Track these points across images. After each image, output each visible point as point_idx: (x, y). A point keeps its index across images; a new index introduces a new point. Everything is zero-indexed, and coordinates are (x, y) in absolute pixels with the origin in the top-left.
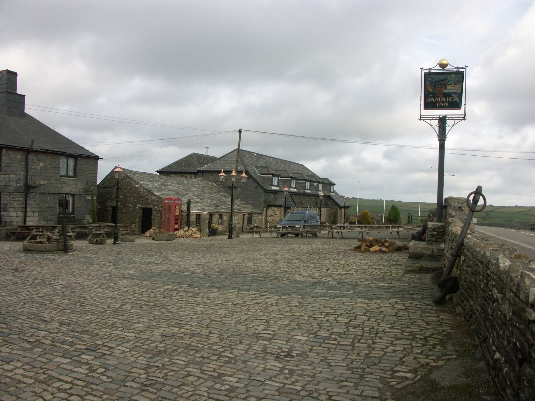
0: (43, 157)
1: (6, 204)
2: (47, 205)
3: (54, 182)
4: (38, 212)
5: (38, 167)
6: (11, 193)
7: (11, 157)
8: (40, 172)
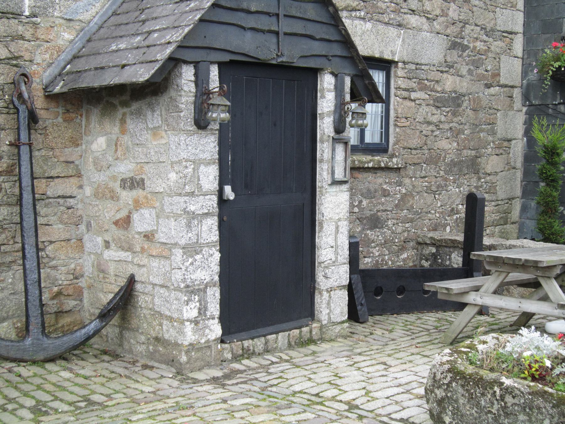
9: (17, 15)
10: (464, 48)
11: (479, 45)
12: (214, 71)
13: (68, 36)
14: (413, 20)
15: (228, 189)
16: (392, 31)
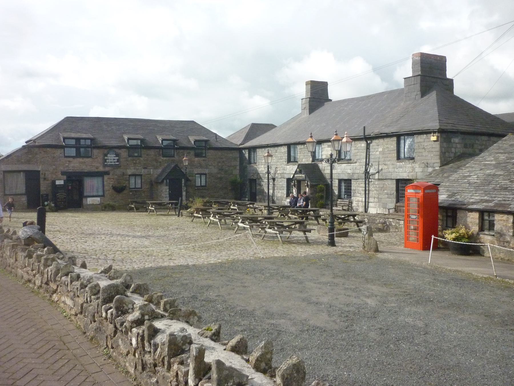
0: (381, 141)
1: (355, 190)
2: (386, 191)
3: (391, 166)
4: (378, 198)
5: (378, 153)
6: (358, 180)
7: (357, 146)
8: (379, 158)
9: (151, 174)
10: (222, 170)
11: (227, 169)
12: (168, 180)
13: (156, 176)
14: (210, 167)
15: (170, 192)
16: (205, 169)
